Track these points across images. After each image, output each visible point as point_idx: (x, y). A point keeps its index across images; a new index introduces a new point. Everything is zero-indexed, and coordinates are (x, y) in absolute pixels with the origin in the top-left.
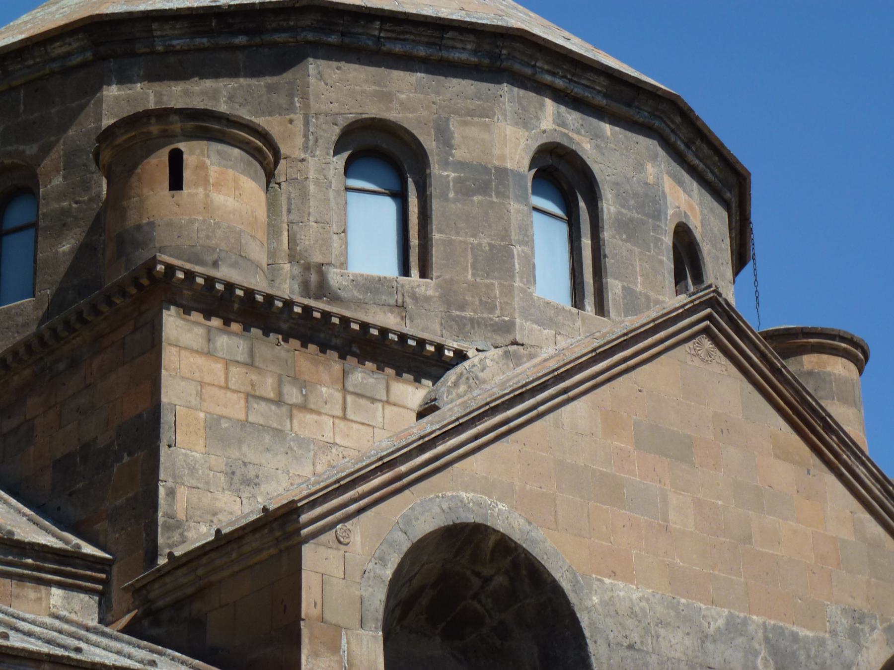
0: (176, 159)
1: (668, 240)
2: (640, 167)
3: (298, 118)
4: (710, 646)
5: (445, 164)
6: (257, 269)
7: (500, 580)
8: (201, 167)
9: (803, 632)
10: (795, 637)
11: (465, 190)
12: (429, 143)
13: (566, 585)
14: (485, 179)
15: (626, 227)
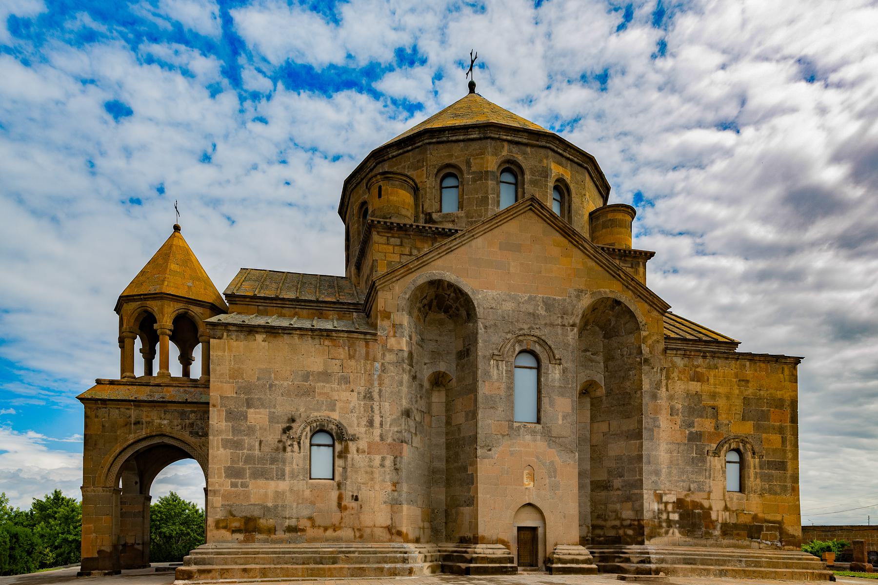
0: (380, 188)
1: (551, 184)
2: (541, 161)
3: (425, 169)
4: (521, 305)
5: (469, 173)
6: (407, 216)
7: (453, 295)
8: (387, 189)
9: (557, 298)
10: (554, 299)
11: (474, 181)
12: (464, 168)
13: (470, 293)
14: (483, 175)
15: (534, 183)
